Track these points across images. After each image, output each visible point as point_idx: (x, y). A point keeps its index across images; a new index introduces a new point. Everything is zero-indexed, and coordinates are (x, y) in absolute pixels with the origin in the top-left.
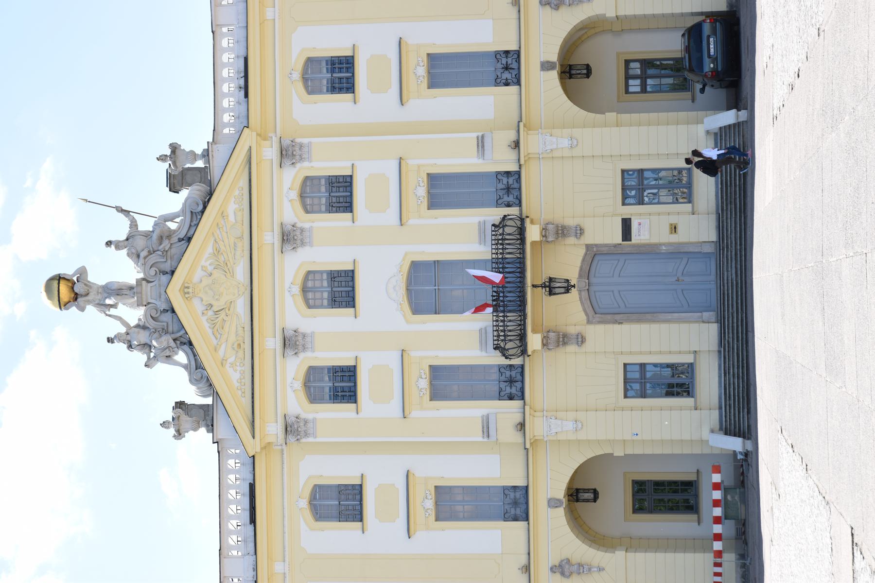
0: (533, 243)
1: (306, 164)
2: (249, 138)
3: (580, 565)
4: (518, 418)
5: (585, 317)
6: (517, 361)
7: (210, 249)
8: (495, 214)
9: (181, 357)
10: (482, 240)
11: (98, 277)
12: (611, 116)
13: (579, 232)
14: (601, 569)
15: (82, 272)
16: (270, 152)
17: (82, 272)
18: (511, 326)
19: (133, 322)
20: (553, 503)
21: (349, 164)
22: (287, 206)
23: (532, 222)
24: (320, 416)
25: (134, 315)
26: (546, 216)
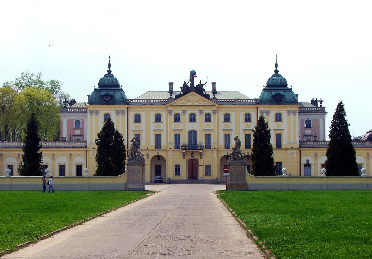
0: (199, 151)
1: (213, 115)
2: (217, 105)
3: (148, 157)
4: (172, 148)
5: (187, 158)
6: (181, 148)
7: (199, 98)
8: (204, 145)
9: (182, 93)
10: (200, 143)
11: (195, 79)
12: (219, 163)
13: (201, 158)
14: (148, 161)
15: (196, 77)
16: (215, 109)
17: (196, 77)
18: (186, 148)
19: (188, 85)
20: (158, 153)
21: (213, 121)
22: (206, 111)
23: (202, 151)
24: (172, 116)
25: (189, 85)
26: (203, 153)
